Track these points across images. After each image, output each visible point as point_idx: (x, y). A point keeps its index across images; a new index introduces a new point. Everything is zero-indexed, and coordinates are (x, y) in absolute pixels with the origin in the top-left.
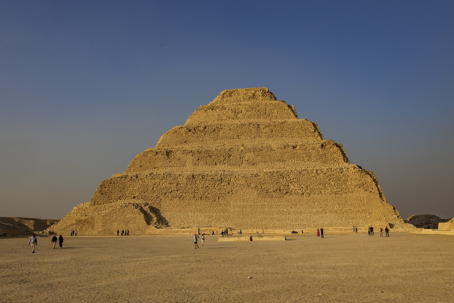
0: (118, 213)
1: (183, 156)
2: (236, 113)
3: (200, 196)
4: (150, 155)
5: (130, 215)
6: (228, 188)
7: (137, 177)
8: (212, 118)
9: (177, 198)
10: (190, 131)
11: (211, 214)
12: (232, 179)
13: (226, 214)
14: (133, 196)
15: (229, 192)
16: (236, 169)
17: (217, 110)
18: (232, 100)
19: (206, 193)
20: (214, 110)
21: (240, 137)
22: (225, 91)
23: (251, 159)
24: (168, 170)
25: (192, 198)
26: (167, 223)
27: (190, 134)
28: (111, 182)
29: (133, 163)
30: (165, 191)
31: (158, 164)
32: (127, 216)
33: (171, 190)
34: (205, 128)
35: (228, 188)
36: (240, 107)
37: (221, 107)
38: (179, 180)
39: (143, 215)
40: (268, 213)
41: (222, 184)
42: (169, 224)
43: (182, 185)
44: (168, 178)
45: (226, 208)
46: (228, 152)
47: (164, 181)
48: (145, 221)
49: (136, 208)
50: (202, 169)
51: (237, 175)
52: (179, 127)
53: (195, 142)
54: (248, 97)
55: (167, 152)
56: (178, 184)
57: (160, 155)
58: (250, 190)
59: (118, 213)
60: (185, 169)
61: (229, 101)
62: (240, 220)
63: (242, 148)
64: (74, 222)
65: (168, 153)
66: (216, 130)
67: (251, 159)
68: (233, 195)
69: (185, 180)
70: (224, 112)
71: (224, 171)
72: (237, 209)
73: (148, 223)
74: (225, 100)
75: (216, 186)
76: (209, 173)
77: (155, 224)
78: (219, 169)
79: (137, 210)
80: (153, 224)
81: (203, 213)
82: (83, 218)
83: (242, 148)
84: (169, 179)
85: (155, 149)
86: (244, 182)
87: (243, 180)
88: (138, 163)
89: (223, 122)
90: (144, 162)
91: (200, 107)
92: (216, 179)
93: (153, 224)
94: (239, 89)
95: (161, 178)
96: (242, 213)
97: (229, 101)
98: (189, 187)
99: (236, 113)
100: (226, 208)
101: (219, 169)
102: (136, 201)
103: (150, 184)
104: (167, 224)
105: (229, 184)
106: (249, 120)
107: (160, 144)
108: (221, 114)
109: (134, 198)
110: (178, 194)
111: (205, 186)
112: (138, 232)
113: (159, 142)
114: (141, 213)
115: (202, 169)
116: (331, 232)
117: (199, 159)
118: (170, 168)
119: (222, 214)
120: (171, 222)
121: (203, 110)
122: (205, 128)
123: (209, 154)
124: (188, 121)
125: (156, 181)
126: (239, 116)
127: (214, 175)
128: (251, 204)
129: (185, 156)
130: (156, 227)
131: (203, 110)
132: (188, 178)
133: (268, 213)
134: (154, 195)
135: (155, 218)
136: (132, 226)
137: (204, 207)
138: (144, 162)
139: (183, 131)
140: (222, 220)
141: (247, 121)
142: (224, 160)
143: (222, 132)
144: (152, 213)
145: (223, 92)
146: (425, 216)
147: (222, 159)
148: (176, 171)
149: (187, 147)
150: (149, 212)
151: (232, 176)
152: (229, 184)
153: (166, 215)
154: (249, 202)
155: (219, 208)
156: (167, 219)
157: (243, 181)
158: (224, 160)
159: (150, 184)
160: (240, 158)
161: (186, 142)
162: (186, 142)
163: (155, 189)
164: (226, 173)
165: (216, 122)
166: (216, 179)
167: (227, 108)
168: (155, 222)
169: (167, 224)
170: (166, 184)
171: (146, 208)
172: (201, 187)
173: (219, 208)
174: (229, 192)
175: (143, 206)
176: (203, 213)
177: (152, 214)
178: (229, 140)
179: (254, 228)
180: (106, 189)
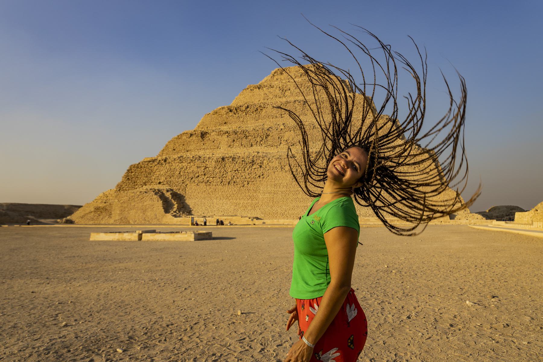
0: (136, 200)
1: (218, 137)
2: (283, 90)
3: (228, 181)
4: (184, 137)
5: (148, 203)
6: (259, 172)
7: (165, 161)
8: (257, 98)
9: (204, 184)
10: (231, 111)
11: (238, 201)
12: (265, 162)
13: (254, 202)
14: (158, 181)
15: (259, 177)
16: (273, 151)
17: (264, 89)
18: (282, 78)
19: (235, 177)
20: (261, 89)
21: (283, 116)
22: (277, 69)
23: (291, 139)
24: (201, 153)
25: (219, 183)
26: (190, 211)
27: (231, 114)
28: (138, 166)
29: (167, 146)
30: (191, 175)
31: (191, 147)
32: (145, 204)
33: (197, 174)
34: (248, 107)
35: (259, 172)
36: (288, 84)
37: (268, 86)
38: (207, 163)
39: (161, 202)
40: (302, 200)
41: (254, 167)
42: (193, 212)
43: (210, 169)
44: (196, 161)
45: (255, 194)
46: (266, 132)
47: (192, 164)
48: (164, 208)
49: (156, 194)
50: (239, 151)
51: (271, 157)
52: (221, 107)
53: (235, 122)
54: (300, 74)
55: (201, 133)
56: (206, 168)
57: (194, 137)
58: (284, 173)
59: (136, 200)
60: (219, 151)
61: (279, 80)
62: (269, 208)
63: (282, 127)
64: (93, 210)
65: (203, 135)
66: (259, 109)
67: (291, 139)
68: (264, 179)
69: (214, 163)
70: (271, 90)
71: (258, 153)
72: (267, 195)
73: (167, 211)
74: (275, 79)
75: (246, 169)
76: (241, 155)
77: (175, 212)
78: (252, 151)
79: (155, 196)
80: (172, 212)
81: (229, 200)
82: (102, 205)
83: (282, 127)
84: (198, 163)
85: (191, 130)
86: (277, 164)
87: (277, 162)
88: (171, 146)
89: (269, 101)
90: (177, 145)
91: (248, 87)
92: (247, 160)
93: (172, 212)
94: (291, 67)
95: (189, 161)
96: (272, 200)
97: (279, 80)
98: (217, 170)
99: (283, 90)
100: (255, 194)
101: (252, 151)
102: (161, 187)
103: (177, 168)
104: (189, 212)
105: (261, 167)
106: (297, 97)
107: (199, 127)
108: (267, 93)
109: (160, 183)
110: (205, 179)
111: (234, 169)
112: (155, 221)
113: (198, 124)
114: (159, 199)
115: (239, 151)
116: (372, 223)
117: (234, 141)
118: (203, 151)
119: (250, 201)
120: (194, 210)
121: (249, 89)
122: (248, 107)
123: (245, 135)
124: (234, 101)
125: (184, 164)
126: (286, 94)
127: (245, 157)
128: (284, 189)
129: (220, 137)
130: (173, 216)
131: (249, 89)
132: (217, 161)
133: (302, 200)
134: (179, 180)
135: (176, 206)
136: (149, 214)
137: (231, 193)
138: (177, 145)
139: (223, 112)
140: (250, 208)
141: (292, 99)
142: (261, 141)
143: (264, 111)
144: (174, 200)
145: (273, 72)
146: (507, 207)
147: (259, 139)
148: (207, 153)
149: (225, 128)
150: (170, 198)
151: (266, 158)
152: (261, 167)
153: (190, 202)
154: (282, 187)
155: (247, 195)
156: (191, 207)
157: (276, 164)
158: (261, 141)
159: (177, 168)
160: (279, 138)
161: (225, 123)
162: (225, 123)
163: (182, 174)
164: (260, 154)
165: (262, 101)
166: (247, 160)
167: (275, 86)
168: (175, 210)
169: (189, 212)
170: (194, 168)
171: (168, 195)
172: (229, 170)
173: (247, 195)
174: (259, 177)
175: (165, 192)
176: (229, 200)
177: (173, 201)
178: (272, 120)
179: (284, 218)
180: (133, 173)
